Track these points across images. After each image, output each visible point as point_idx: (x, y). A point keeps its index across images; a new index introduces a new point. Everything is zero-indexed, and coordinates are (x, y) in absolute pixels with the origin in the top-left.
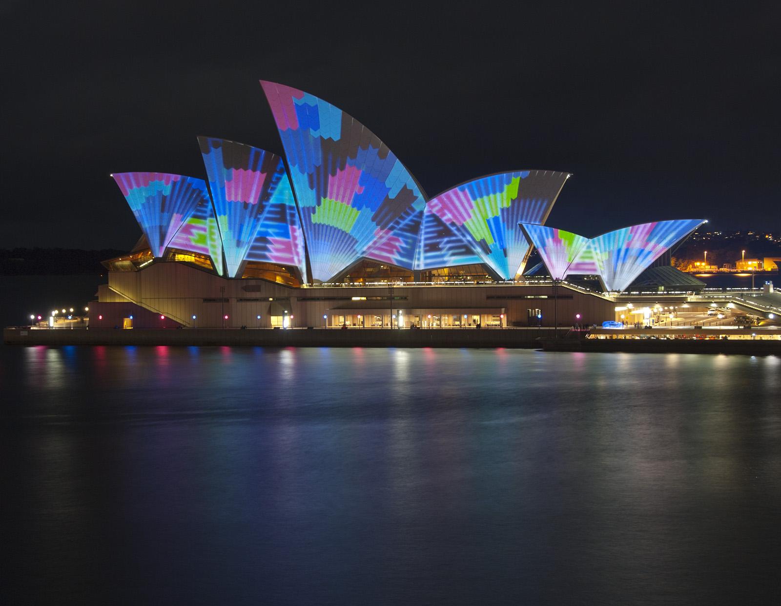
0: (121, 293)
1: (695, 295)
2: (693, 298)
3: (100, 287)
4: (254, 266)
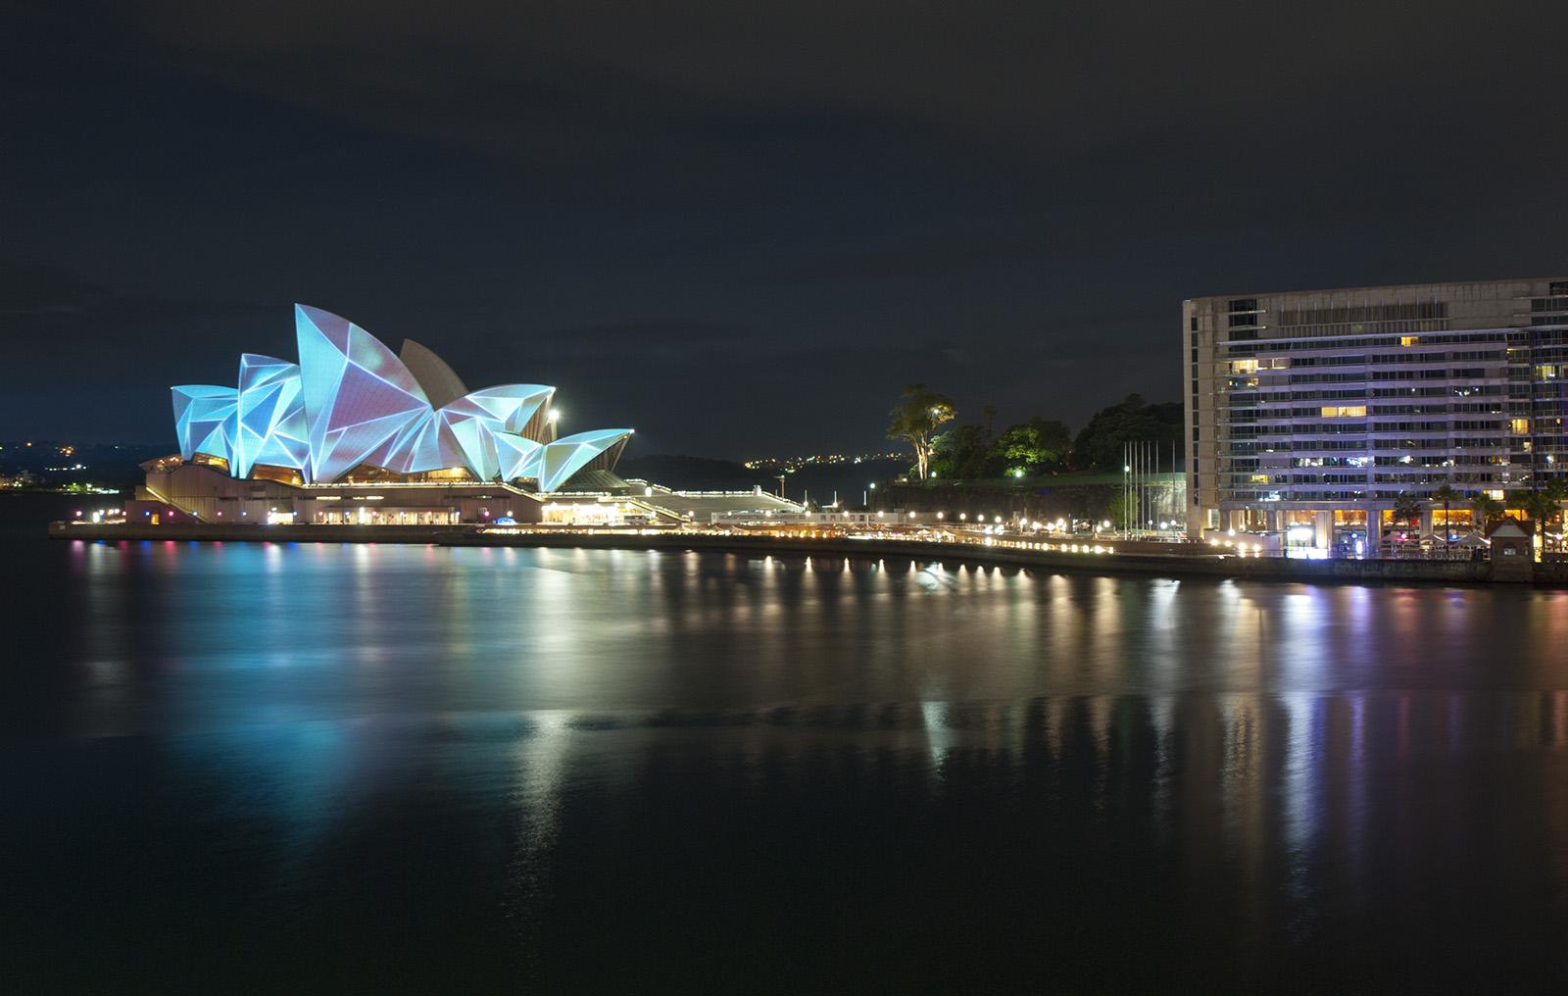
0: (154, 492)
3: (137, 488)
4: (263, 469)
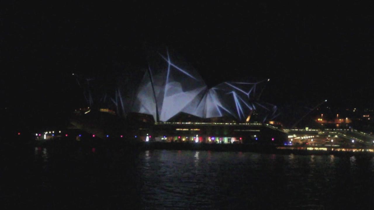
1: (322, 131)
2: (320, 133)
